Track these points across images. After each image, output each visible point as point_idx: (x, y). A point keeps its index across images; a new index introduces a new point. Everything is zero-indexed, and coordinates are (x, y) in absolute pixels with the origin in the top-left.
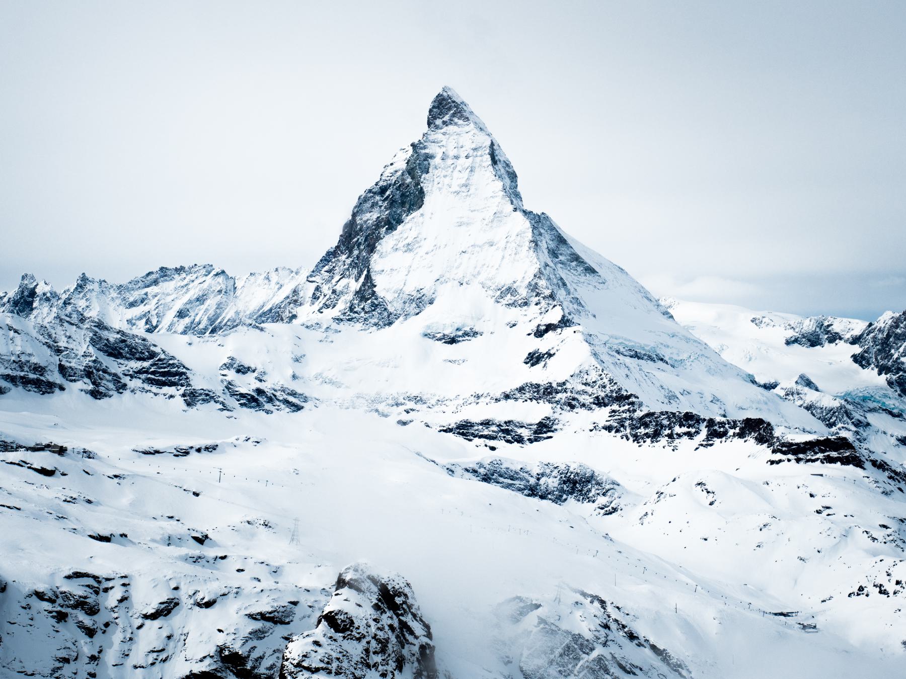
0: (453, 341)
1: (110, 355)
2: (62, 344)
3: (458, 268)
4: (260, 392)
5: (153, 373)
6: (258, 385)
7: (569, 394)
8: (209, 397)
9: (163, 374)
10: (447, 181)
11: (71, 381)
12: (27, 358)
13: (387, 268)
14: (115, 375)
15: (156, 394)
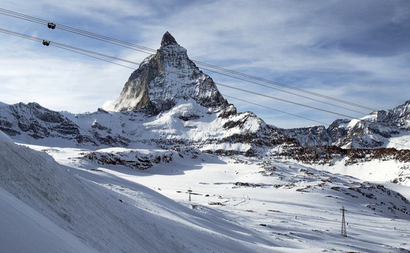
0: (186, 119)
1: (42, 119)
2: (20, 114)
3: (182, 92)
4: (109, 137)
5: (62, 128)
6: (109, 134)
7: (259, 139)
8: (88, 140)
9: (66, 129)
10: (172, 63)
11: (24, 131)
12: (3, 119)
13: (153, 92)
14: (45, 128)
15: (63, 138)
